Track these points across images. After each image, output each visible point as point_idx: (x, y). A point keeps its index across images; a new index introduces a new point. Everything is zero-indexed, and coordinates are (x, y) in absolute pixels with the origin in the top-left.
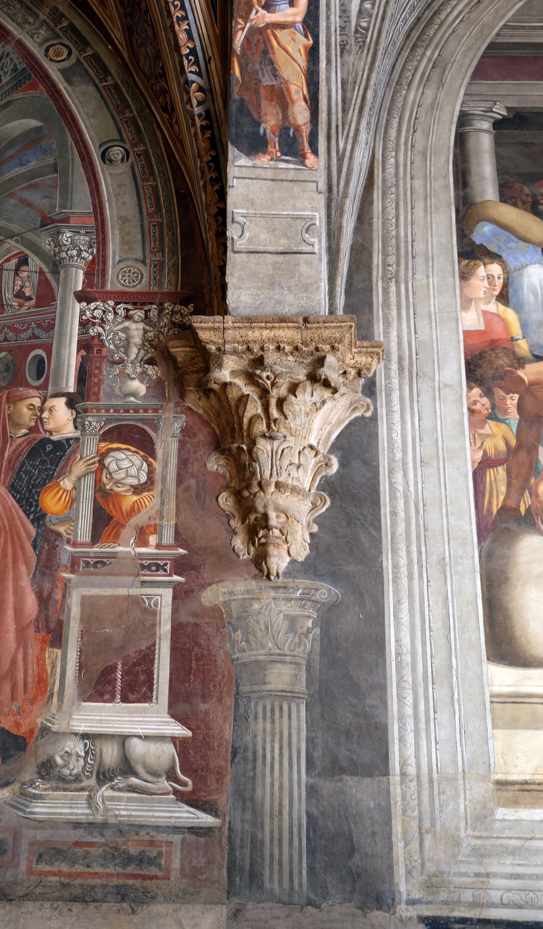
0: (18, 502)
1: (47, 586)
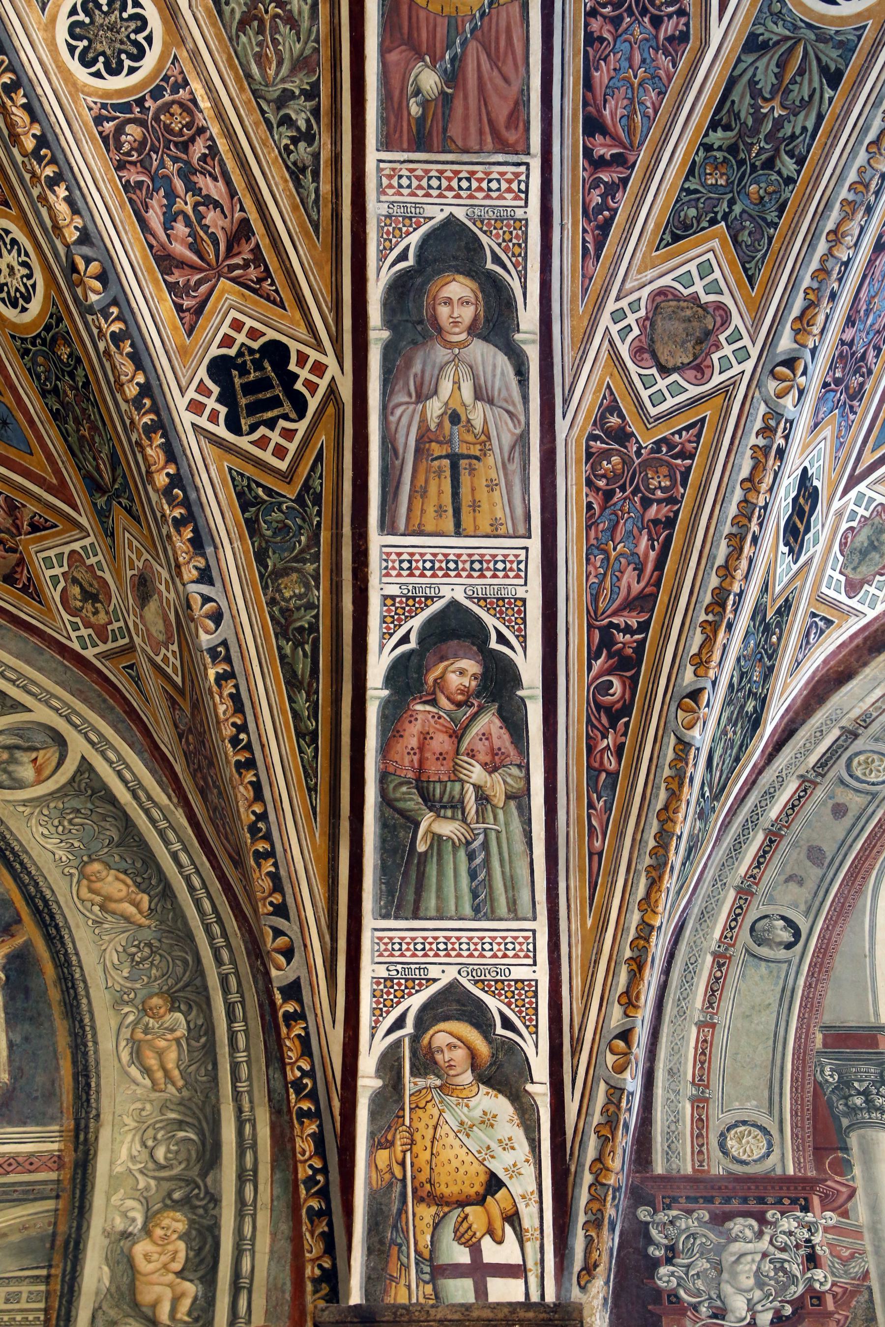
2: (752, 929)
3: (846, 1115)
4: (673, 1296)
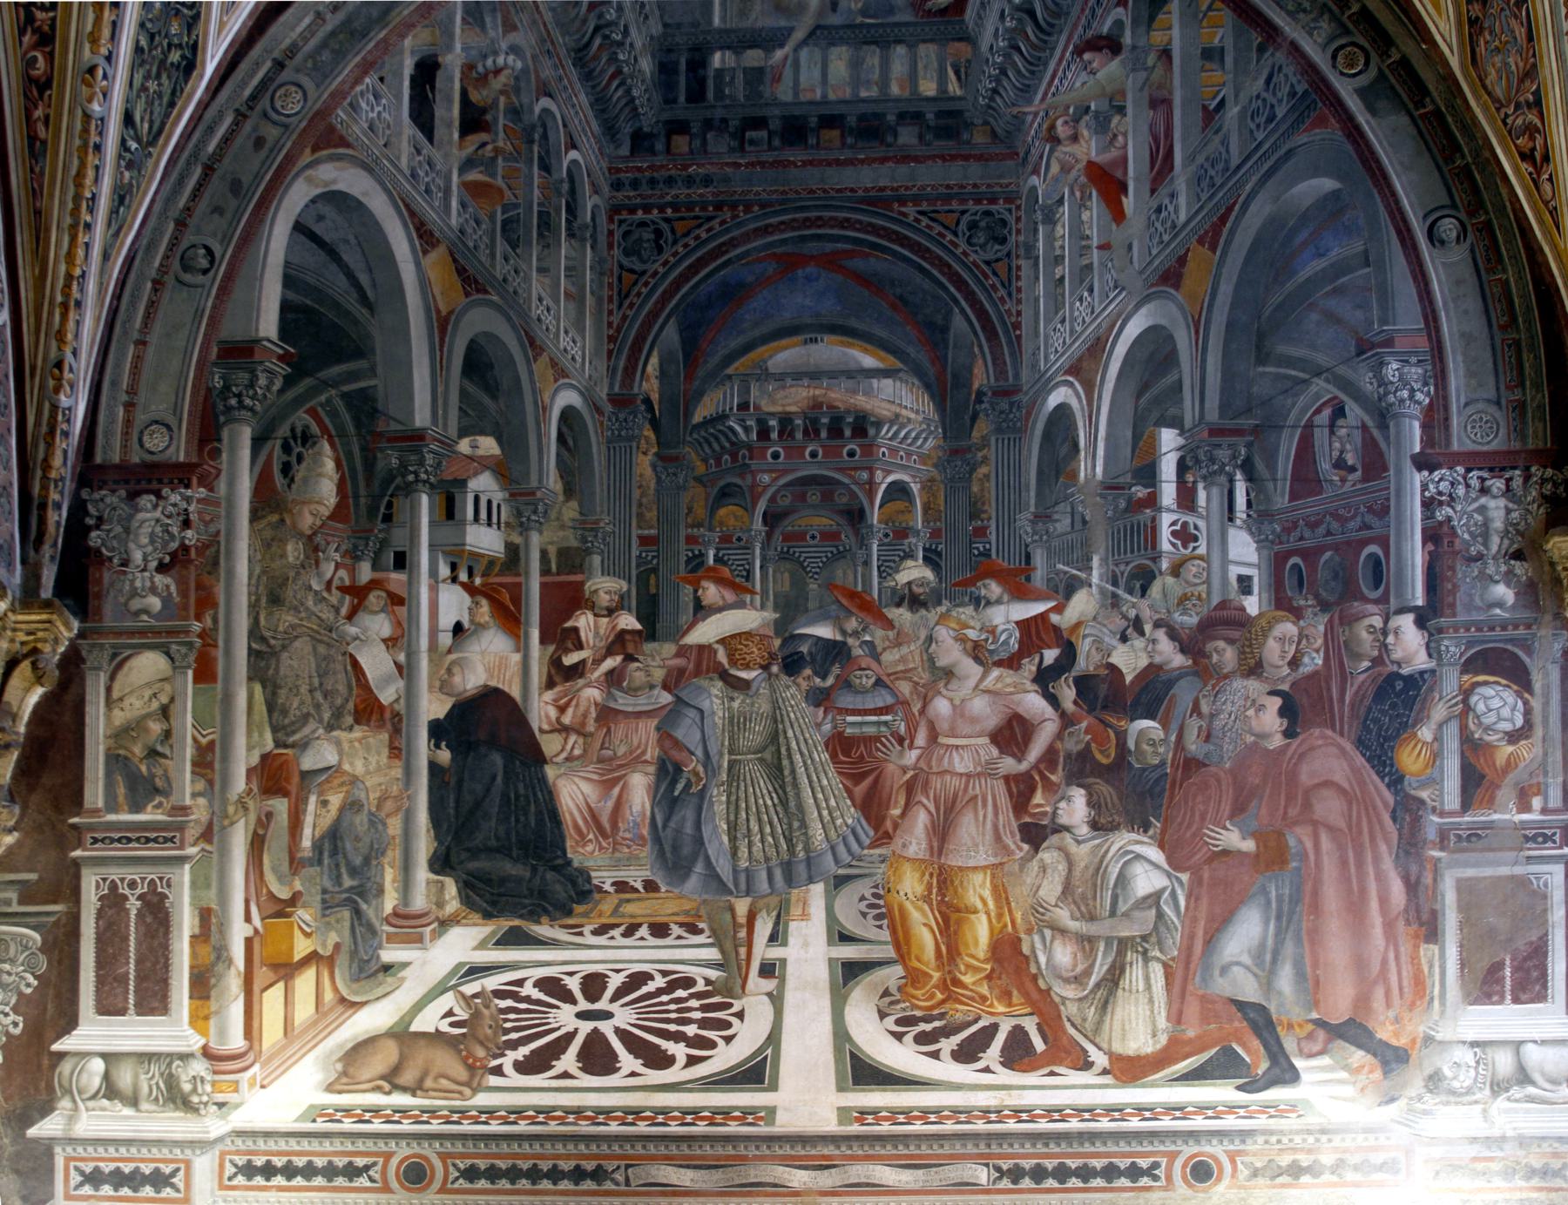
0: (1368, 760)
1: (1414, 869)
2: (182, 258)
3: (223, 413)
4: (98, 551)
